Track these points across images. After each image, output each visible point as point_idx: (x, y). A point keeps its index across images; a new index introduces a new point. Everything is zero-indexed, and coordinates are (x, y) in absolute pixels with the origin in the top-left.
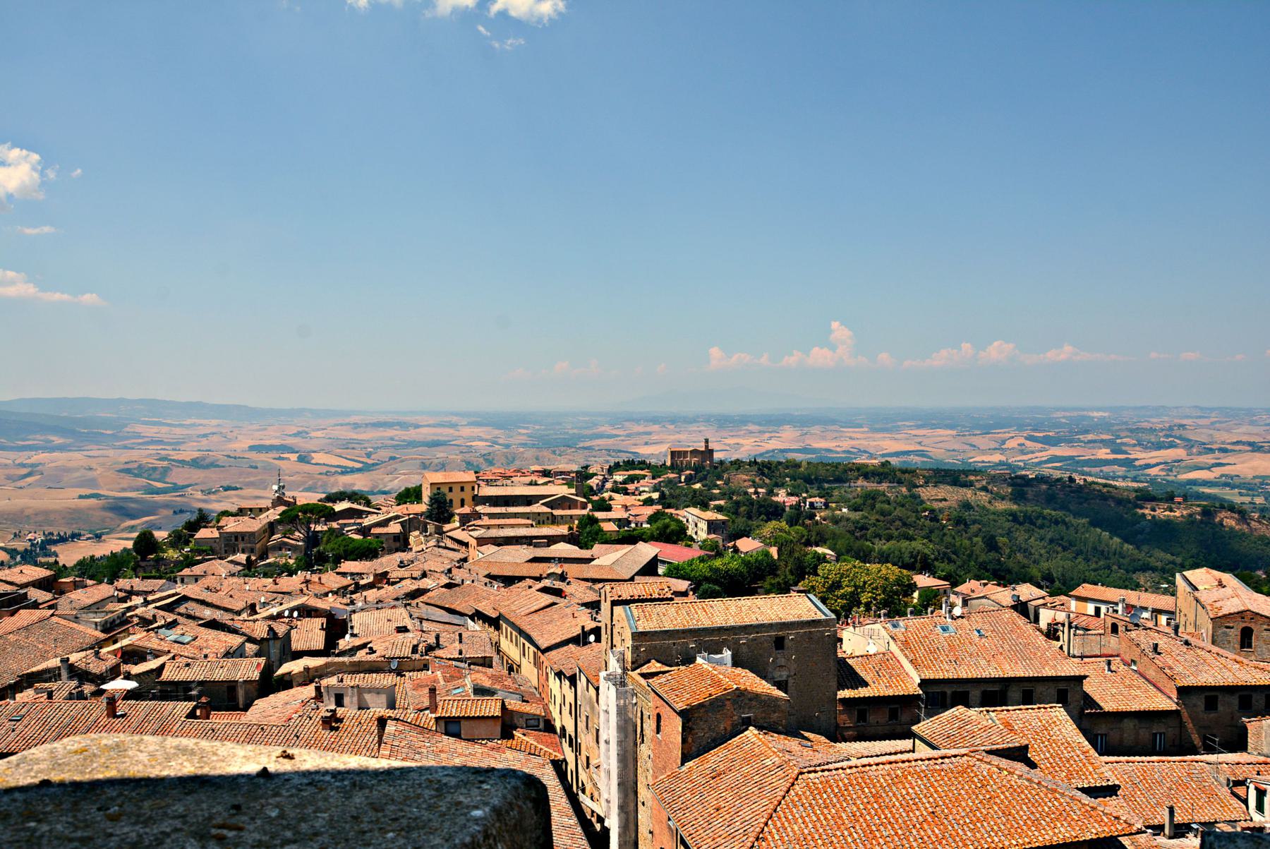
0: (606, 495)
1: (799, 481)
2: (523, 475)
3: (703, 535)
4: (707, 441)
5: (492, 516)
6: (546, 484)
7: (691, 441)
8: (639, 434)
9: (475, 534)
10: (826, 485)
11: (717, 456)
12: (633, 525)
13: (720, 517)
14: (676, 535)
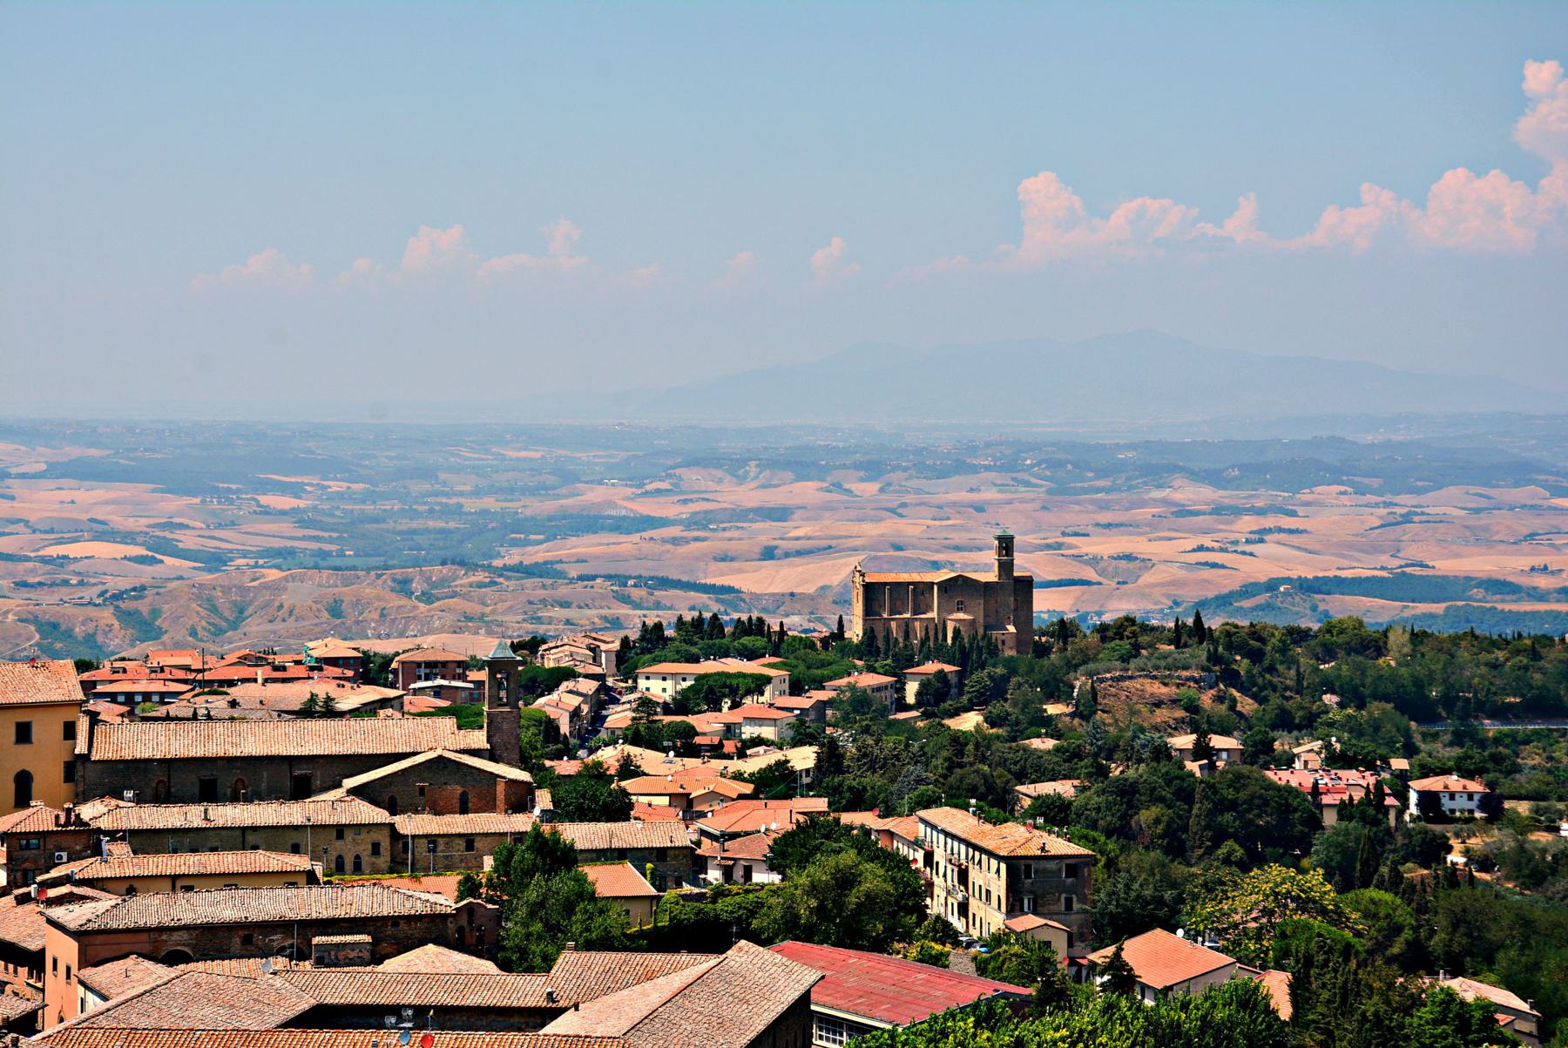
0: (609, 756)
1: (1376, 709)
2: (280, 675)
3: (992, 918)
4: (1006, 545)
5: (144, 841)
6: (368, 710)
7: (946, 542)
8: (740, 515)
9: (73, 915)
10: (1491, 728)
11: (1046, 605)
12: (714, 875)
13: (1059, 846)
14: (878, 913)
